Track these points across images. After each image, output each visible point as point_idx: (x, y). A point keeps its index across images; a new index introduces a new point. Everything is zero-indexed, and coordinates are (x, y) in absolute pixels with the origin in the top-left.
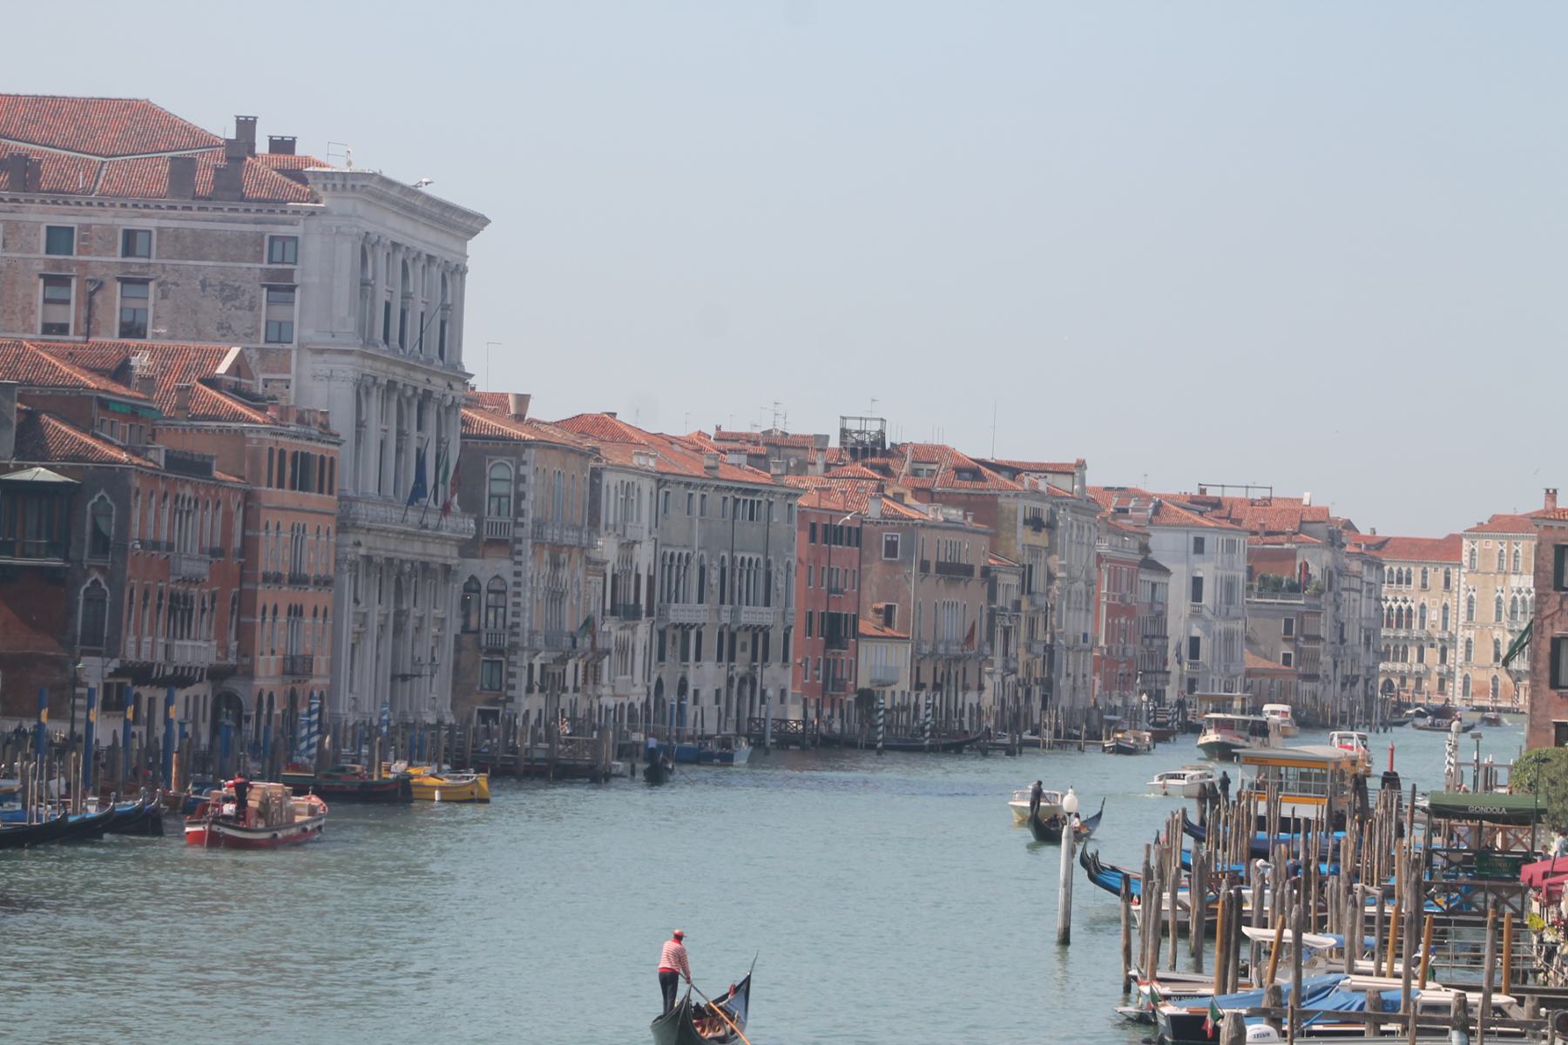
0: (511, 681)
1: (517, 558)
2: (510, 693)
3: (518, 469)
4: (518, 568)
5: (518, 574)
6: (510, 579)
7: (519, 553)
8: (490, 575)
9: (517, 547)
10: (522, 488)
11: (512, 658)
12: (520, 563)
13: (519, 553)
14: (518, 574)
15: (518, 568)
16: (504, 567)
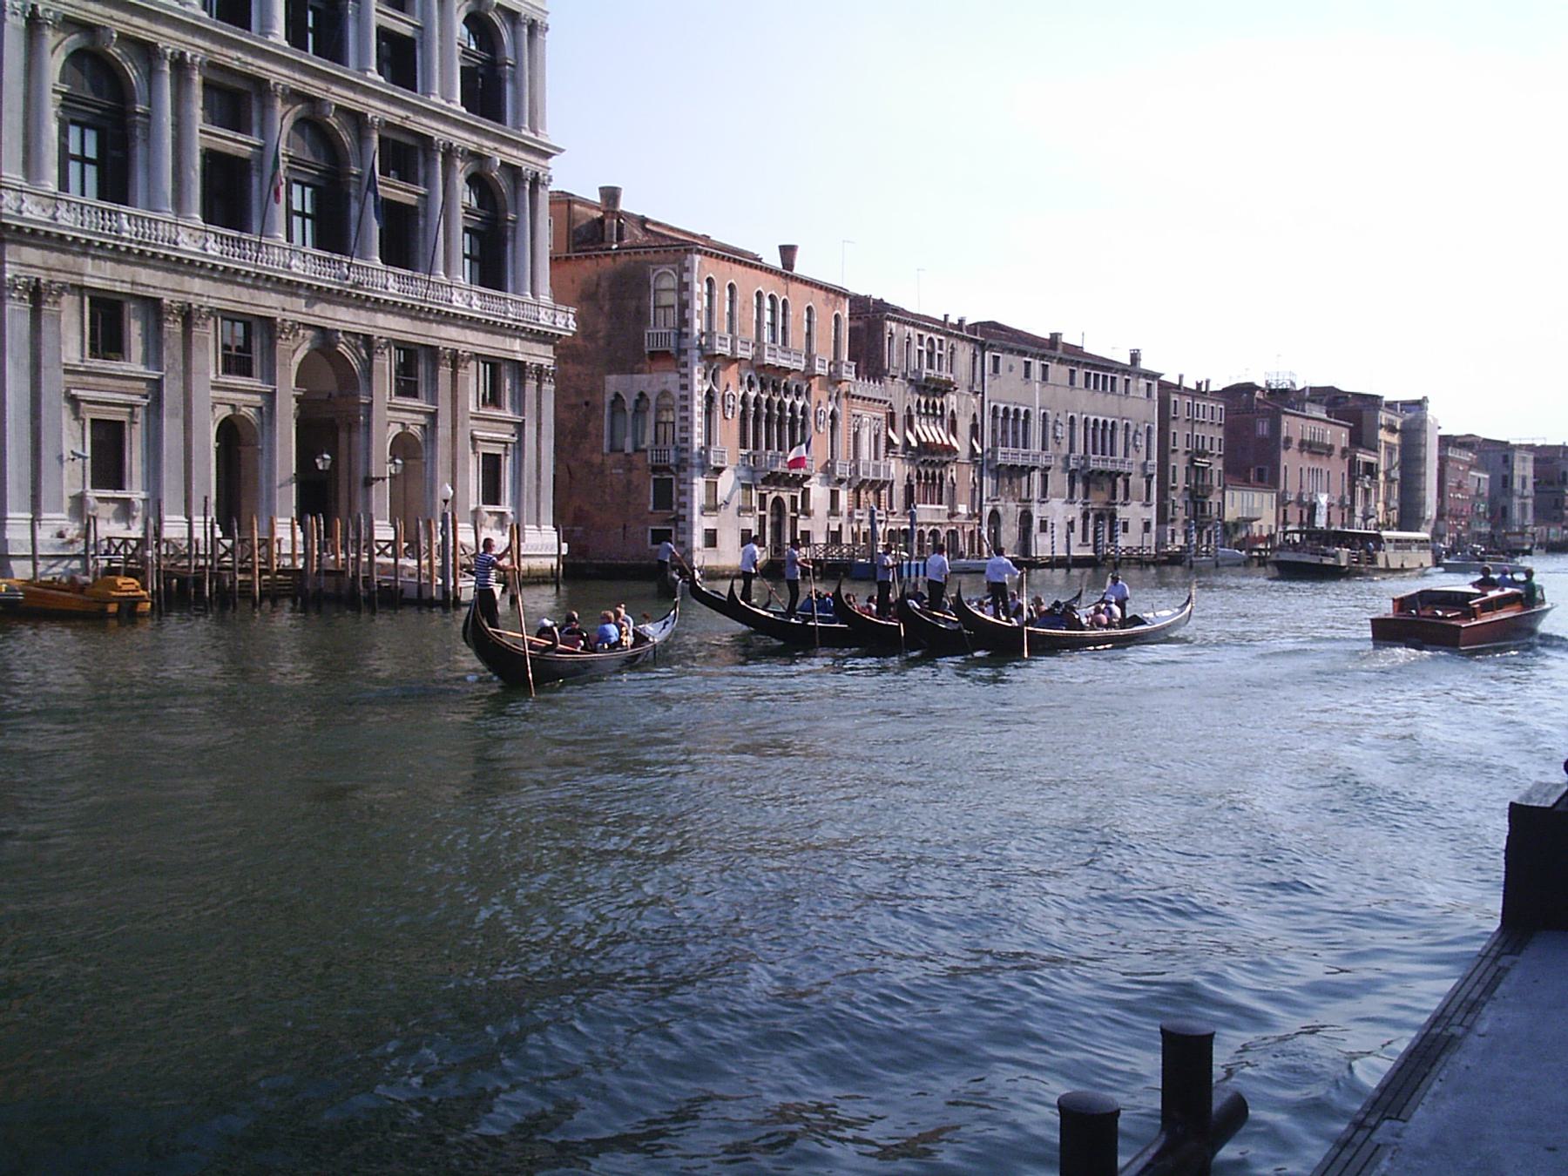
0: (682, 499)
1: (683, 371)
2: (681, 512)
3: (680, 277)
4: (684, 381)
5: (684, 387)
6: (676, 392)
7: (685, 365)
8: (658, 389)
9: (683, 359)
10: (685, 295)
11: (682, 475)
12: (686, 375)
13: (685, 365)
14: (684, 387)
15: (684, 381)
16: (671, 380)
